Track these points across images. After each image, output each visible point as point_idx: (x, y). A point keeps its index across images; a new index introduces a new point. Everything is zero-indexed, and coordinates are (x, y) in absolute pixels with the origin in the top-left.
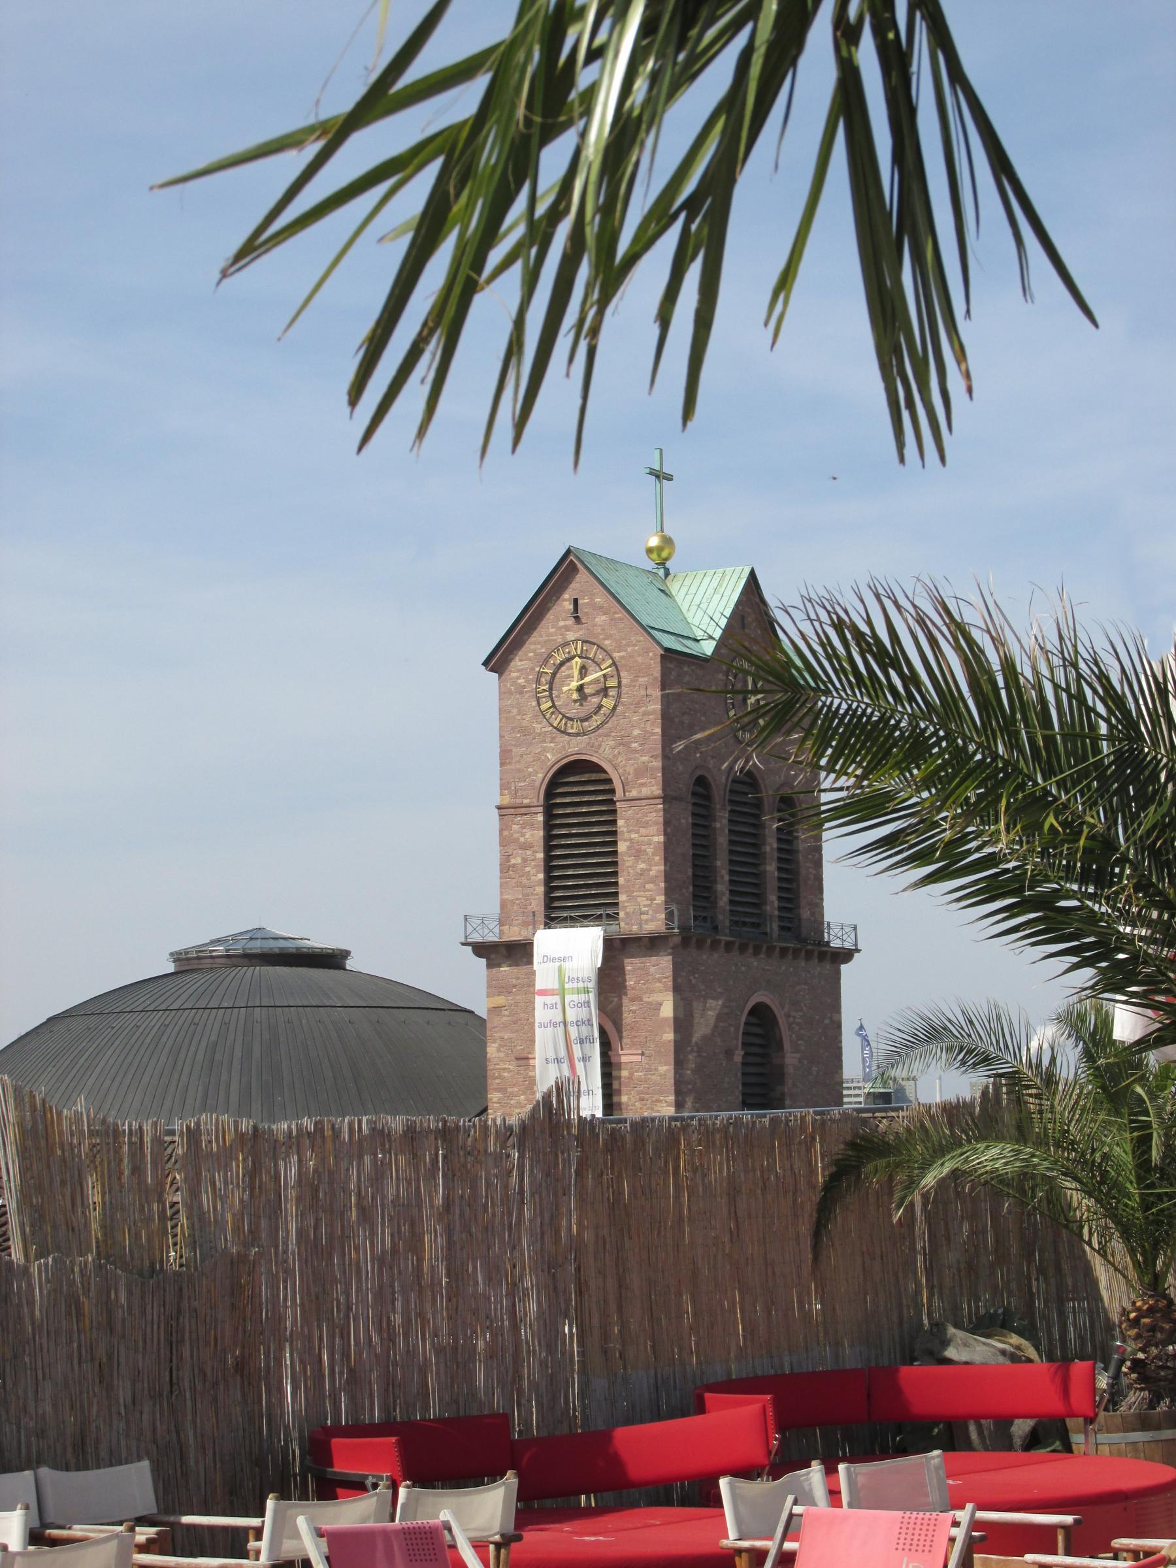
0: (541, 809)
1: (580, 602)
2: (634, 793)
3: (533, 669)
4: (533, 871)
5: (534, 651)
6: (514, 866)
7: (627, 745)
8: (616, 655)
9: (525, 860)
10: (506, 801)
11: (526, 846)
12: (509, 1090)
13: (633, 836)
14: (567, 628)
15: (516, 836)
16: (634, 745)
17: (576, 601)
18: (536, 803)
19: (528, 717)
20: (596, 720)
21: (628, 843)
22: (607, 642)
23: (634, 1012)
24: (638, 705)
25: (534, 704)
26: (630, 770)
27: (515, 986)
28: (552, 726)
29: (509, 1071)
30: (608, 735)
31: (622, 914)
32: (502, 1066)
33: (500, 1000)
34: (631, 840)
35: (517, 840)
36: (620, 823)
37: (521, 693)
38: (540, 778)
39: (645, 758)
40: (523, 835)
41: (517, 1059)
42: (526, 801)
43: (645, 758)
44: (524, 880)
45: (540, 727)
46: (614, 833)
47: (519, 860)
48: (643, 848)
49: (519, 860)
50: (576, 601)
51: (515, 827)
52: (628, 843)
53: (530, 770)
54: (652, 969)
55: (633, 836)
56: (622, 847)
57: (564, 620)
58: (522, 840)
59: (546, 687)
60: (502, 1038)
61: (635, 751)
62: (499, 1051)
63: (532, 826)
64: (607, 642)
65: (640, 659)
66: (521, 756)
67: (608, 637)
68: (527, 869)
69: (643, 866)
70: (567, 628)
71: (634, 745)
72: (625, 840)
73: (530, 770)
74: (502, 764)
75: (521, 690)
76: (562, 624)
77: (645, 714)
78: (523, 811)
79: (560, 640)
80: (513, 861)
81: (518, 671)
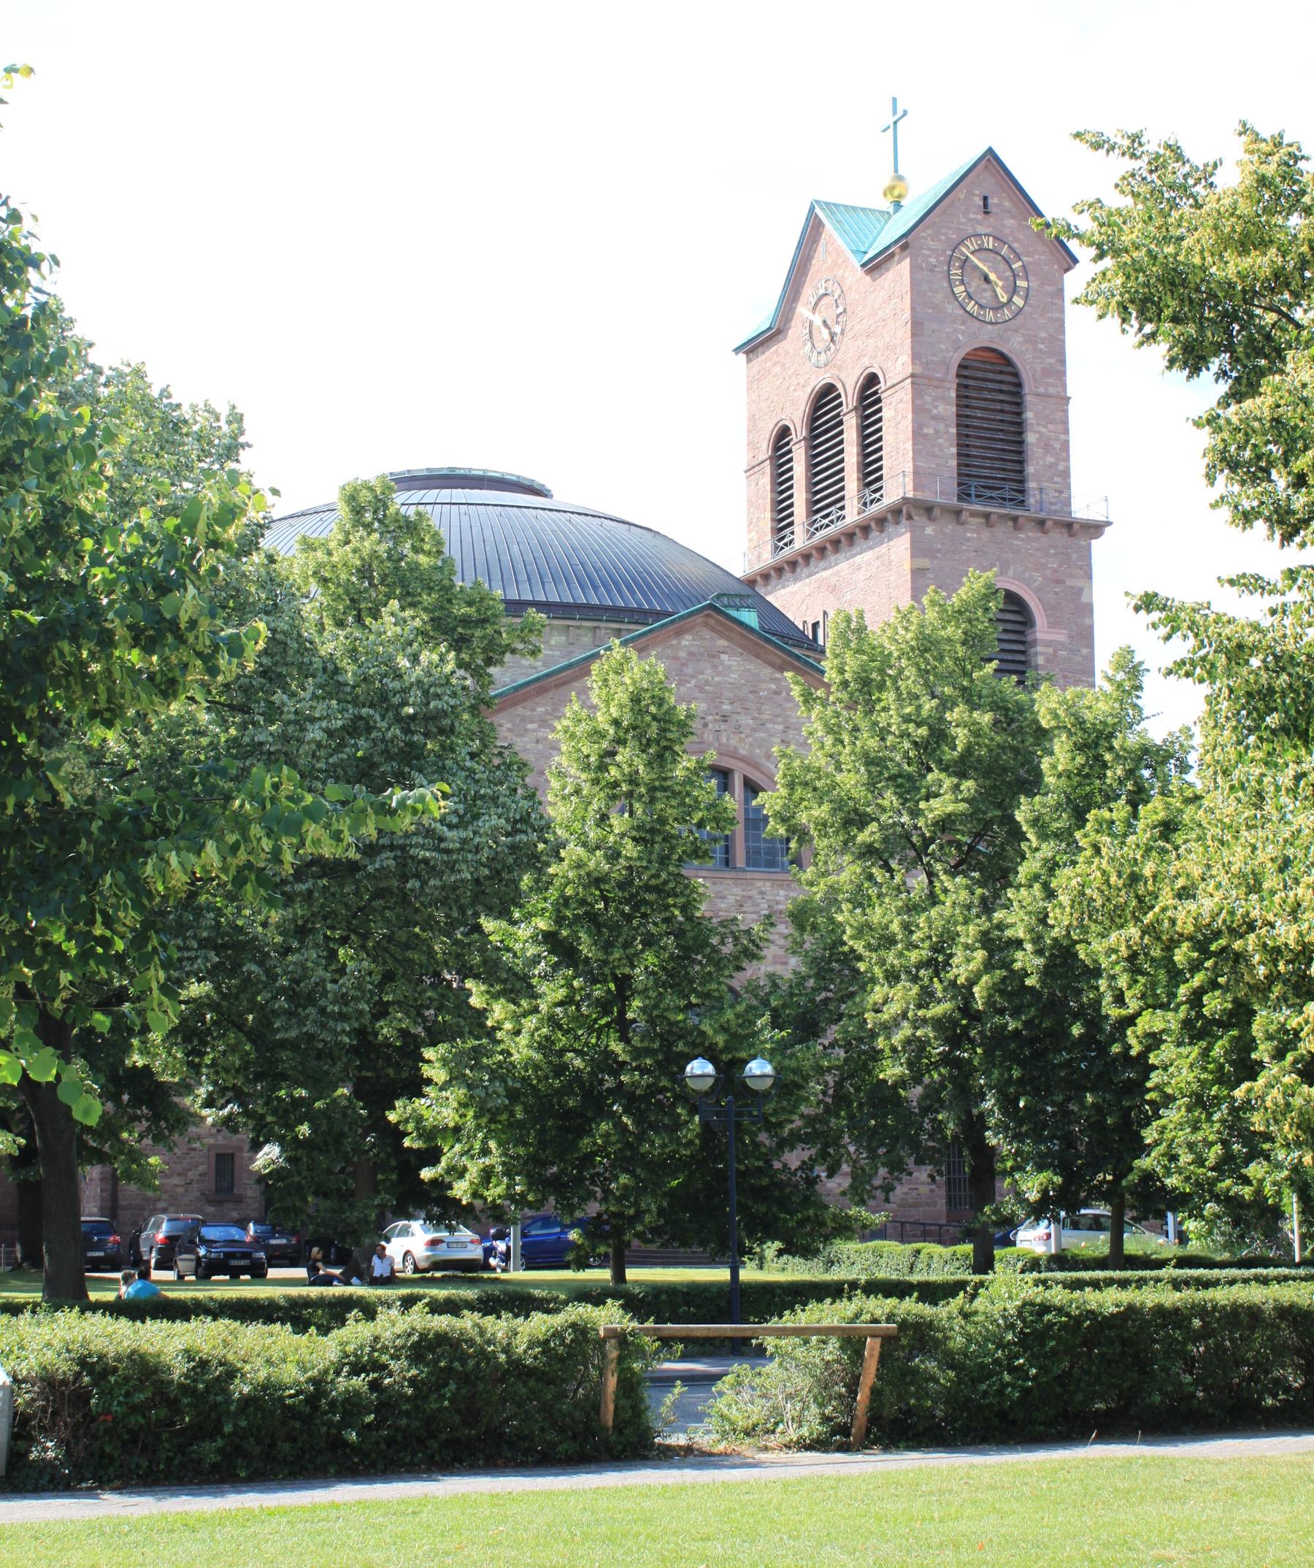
1: (990, 201)
2: (1042, 390)
4: (946, 444)
5: (945, 234)
9: (936, 431)
10: (919, 370)
11: (936, 418)
14: (978, 222)
15: (929, 407)
16: (1041, 346)
17: (985, 199)
22: (1015, 245)
23: (1057, 593)
26: (1039, 369)
27: (939, 551)
30: (1016, 331)
33: (925, 563)
35: (928, 411)
37: (931, 271)
38: (956, 358)
39: (1052, 361)
40: (936, 407)
43: (1052, 361)
45: (952, 308)
47: (932, 431)
49: (932, 431)
50: (985, 199)
51: (928, 399)
53: (943, 347)
56: (1030, 438)
57: (975, 213)
58: (934, 411)
61: (1041, 351)
65: (1046, 269)
67: (1017, 240)
68: (940, 441)
70: (978, 222)
71: (1041, 346)
76: (972, 216)
78: (936, 383)
79: (971, 231)
80: (926, 431)
81: (930, 249)
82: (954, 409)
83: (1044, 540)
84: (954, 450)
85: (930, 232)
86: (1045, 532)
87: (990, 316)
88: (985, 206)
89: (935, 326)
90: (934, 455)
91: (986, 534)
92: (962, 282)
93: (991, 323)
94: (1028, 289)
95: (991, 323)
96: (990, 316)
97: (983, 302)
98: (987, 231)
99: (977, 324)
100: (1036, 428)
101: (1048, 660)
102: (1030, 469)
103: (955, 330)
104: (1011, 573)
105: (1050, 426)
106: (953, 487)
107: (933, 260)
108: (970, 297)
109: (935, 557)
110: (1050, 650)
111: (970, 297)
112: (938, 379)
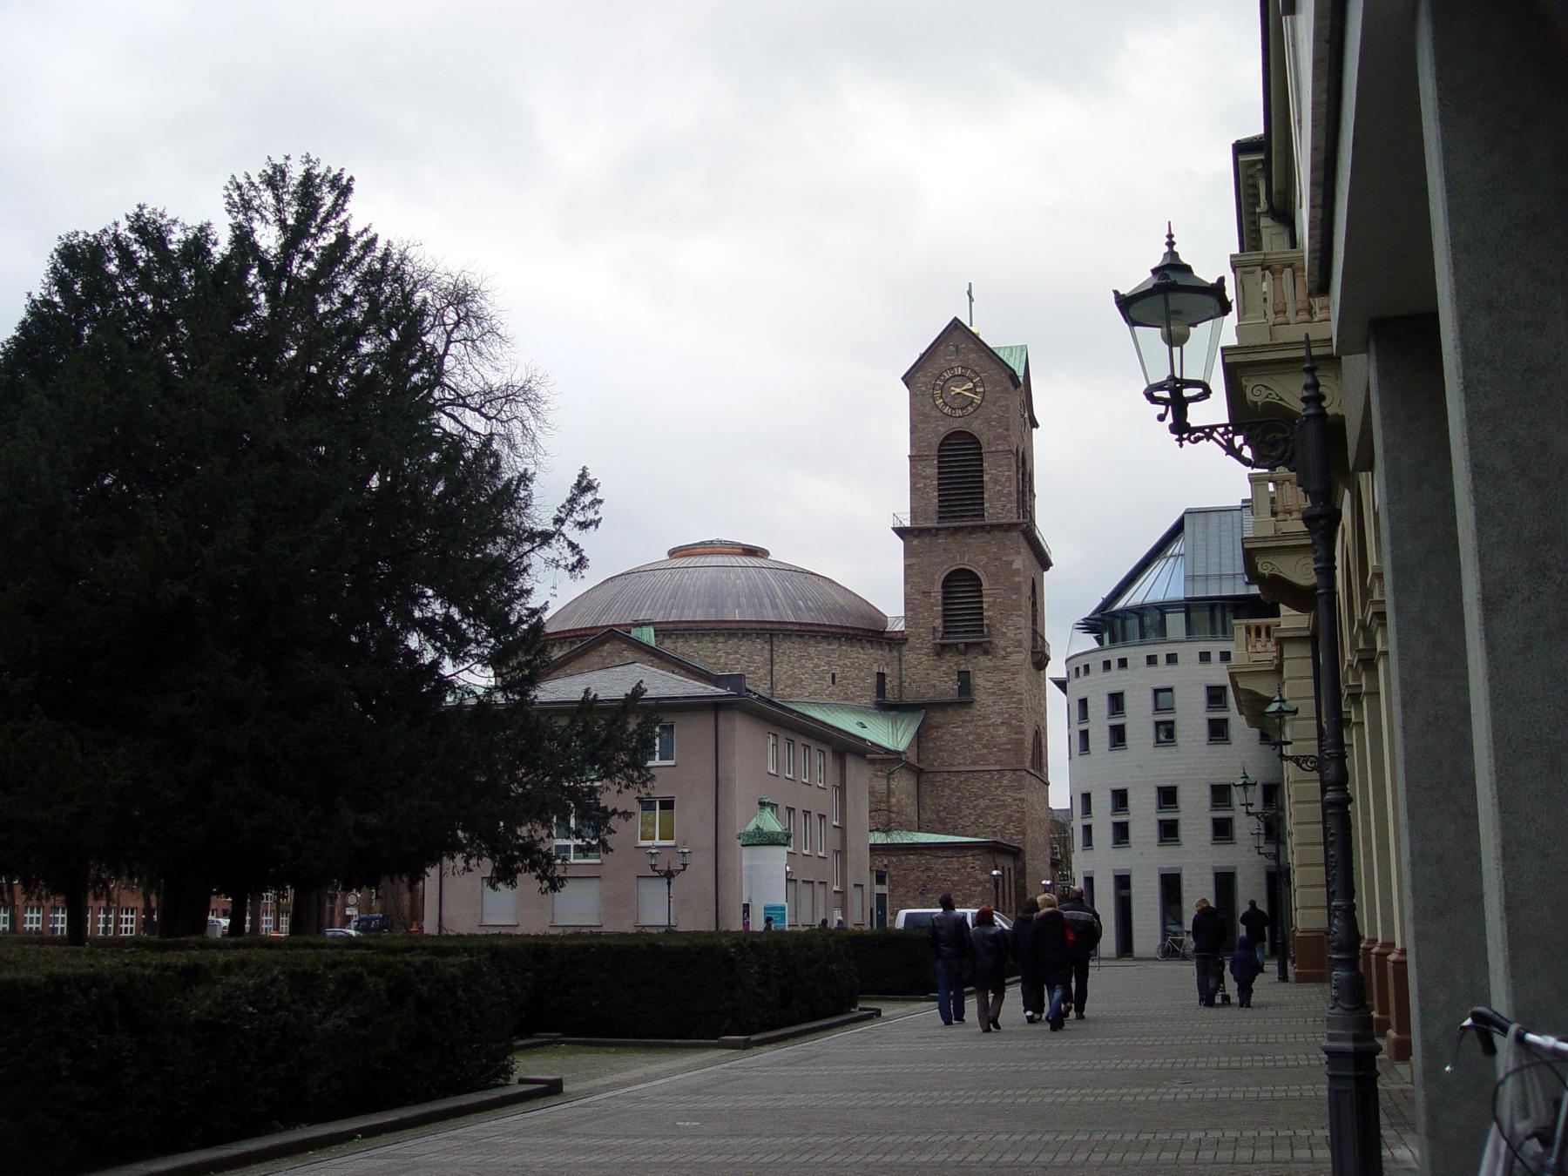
0: (936, 457)
2: (993, 449)
3: (930, 382)
6: (918, 488)
7: (989, 423)
8: (982, 375)
9: (925, 485)
10: (914, 454)
11: (926, 478)
12: (918, 610)
13: (994, 471)
18: (932, 454)
19: (928, 408)
20: (970, 409)
21: (989, 476)
22: (977, 368)
23: (996, 566)
24: (995, 402)
25: (931, 401)
28: (942, 412)
29: (917, 599)
30: (977, 418)
31: (986, 514)
32: (913, 597)
34: (992, 474)
35: (920, 475)
36: (985, 465)
37: (923, 395)
38: (936, 441)
39: (1000, 430)
41: (923, 592)
42: (927, 453)
43: (1000, 430)
44: (925, 495)
45: (935, 413)
46: (982, 471)
47: (922, 485)
48: (1000, 478)
49: (922, 485)
50: (957, 346)
51: (920, 467)
52: (989, 476)
54: (1008, 543)
55: (994, 471)
56: (986, 478)
59: (939, 392)
60: (913, 582)
61: (993, 426)
62: (911, 589)
63: (930, 466)
64: (977, 368)
65: (997, 377)
66: (923, 429)
69: (1000, 488)
72: (987, 474)
73: (929, 436)
74: (911, 433)
75: (923, 394)
76: (948, 358)
77: (999, 407)
78: (925, 458)
79: (948, 367)
80: (918, 486)
82: (936, 470)
83: (988, 537)
84: (936, 494)
85: (920, 373)
86: (988, 532)
87: (959, 413)
88: (957, 350)
89: (924, 425)
90: (924, 499)
91: (950, 539)
92: (941, 397)
93: (960, 417)
94: (984, 392)
95: (960, 417)
96: (959, 413)
97: (955, 406)
98: (958, 364)
99: (952, 419)
100: (989, 471)
101: (990, 606)
102: (986, 496)
103: (938, 425)
104: (966, 559)
105: (999, 469)
106: (935, 516)
107: (923, 389)
108: (946, 405)
109: (918, 557)
110: (991, 599)
111: (946, 405)
112: (927, 456)
